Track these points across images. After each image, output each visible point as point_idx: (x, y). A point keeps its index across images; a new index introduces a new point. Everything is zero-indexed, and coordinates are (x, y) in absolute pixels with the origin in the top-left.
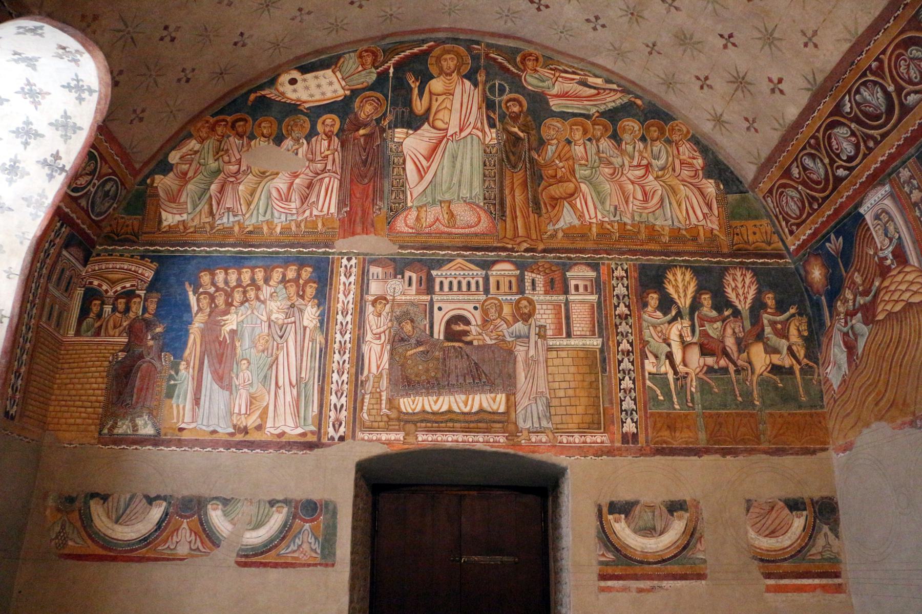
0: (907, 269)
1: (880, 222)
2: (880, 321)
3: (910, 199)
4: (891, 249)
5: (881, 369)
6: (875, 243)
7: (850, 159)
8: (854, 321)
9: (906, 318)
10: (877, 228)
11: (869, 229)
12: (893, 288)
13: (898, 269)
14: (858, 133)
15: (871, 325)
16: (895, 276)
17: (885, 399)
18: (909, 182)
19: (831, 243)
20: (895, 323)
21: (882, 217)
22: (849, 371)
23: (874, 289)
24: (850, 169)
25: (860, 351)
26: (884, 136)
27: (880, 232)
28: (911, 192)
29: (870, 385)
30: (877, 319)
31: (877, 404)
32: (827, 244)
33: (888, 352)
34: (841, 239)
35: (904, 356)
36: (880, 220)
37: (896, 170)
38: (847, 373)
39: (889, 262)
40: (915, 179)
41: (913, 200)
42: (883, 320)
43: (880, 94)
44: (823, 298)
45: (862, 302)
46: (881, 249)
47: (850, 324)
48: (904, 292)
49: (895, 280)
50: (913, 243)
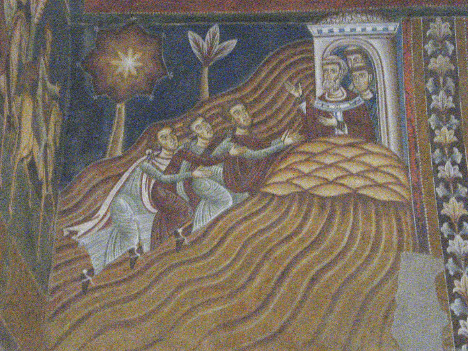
0: (369, 147)
1: (341, 62)
2: (274, 196)
3: (427, 63)
4: (345, 106)
5: (256, 271)
6: (314, 83)
8: (197, 173)
9: (344, 213)
10: (330, 67)
11: (312, 59)
12: (329, 160)
15: (246, 195)
16: (337, 146)
17: (251, 324)
19: (204, 38)
20: (315, 210)
21: (352, 57)
22: (152, 248)
23: (275, 146)
25: (198, 226)
27: (333, 76)
28: (434, 55)
29: (216, 288)
30: (268, 190)
31: (226, 325)
32: (192, 35)
33: (284, 248)
34: (232, 44)
35: (328, 266)
36: (346, 60)
38: (146, 248)
39: (332, 122)
40: (453, 43)
41: (430, 66)
42: (282, 198)
44: (121, 107)
45: (234, 151)
46: (322, 98)
47: (183, 173)
48: (351, 174)
49: (337, 151)
50: (399, 119)
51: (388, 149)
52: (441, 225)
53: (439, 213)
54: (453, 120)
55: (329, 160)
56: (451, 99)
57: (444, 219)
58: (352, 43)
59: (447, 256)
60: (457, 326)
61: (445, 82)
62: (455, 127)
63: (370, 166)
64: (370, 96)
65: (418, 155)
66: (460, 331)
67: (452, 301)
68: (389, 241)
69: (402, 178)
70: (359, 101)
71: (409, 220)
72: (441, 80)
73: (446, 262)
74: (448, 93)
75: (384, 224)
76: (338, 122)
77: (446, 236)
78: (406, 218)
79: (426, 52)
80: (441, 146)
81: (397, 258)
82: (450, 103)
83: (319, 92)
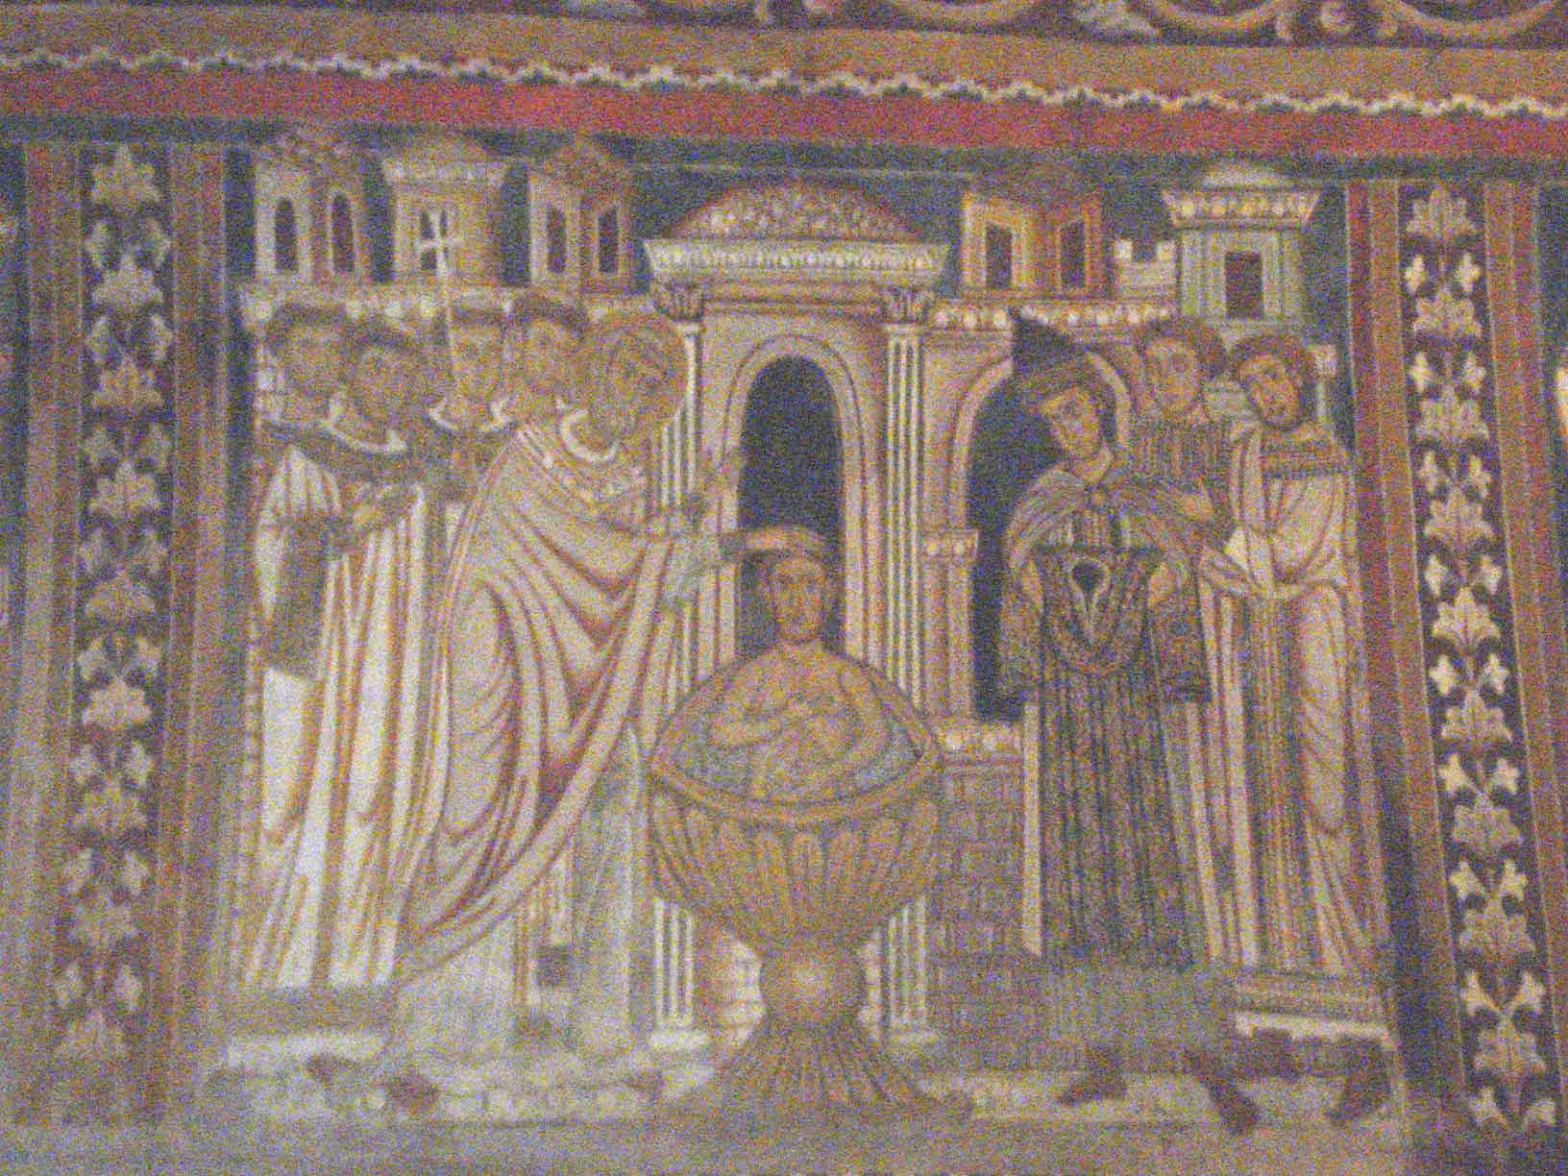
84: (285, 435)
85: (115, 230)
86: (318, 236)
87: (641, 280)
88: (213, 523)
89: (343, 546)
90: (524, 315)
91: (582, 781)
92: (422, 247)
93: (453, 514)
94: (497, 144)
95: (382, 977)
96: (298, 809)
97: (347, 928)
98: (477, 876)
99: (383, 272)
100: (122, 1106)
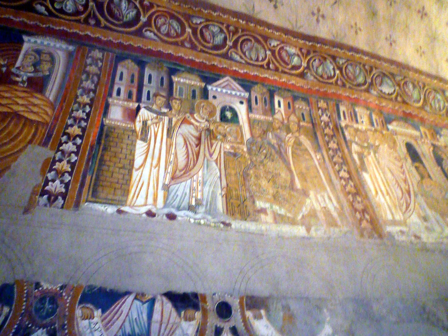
1: (37, 56)
7: (61, 11)
11: (19, 50)
13: (26, 89)
14: (89, 9)
18: (95, 61)
21: (44, 55)
24: (51, 14)
26: (106, 27)
28: (91, 65)
37: (93, 48)
43: (132, 14)
46: (18, 68)
48: (18, 104)
49: (15, 92)
50: (60, 88)
51: (48, 99)
52: (63, 136)
53: (64, 131)
54: (92, 94)
55: (7, 95)
56: (93, 85)
57: (65, 134)
58: (46, 50)
59: (58, 150)
60: (46, 184)
61: (92, 77)
62: (91, 97)
63: (32, 103)
64: (48, 73)
65: (65, 104)
66: (47, 188)
67: (50, 172)
68: (25, 138)
69: (50, 112)
70: (40, 74)
71: (43, 131)
72: (91, 76)
73: (56, 153)
74: (93, 82)
75: (26, 130)
76: (23, 80)
77: (63, 142)
78: (42, 130)
79: (86, 62)
80: (79, 104)
81: (25, 147)
82: (93, 87)
83: (18, 64)
84: (351, 142)
85: (322, 110)
86: (348, 115)
87: (388, 129)
88: (346, 151)
89: (365, 157)
90: (376, 131)
91: (412, 193)
92: (361, 120)
93: (377, 155)
94: (368, 109)
95: (402, 219)
96: (377, 193)
97: (393, 210)
98: (407, 206)
99: (357, 121)
100: (376, 235)
